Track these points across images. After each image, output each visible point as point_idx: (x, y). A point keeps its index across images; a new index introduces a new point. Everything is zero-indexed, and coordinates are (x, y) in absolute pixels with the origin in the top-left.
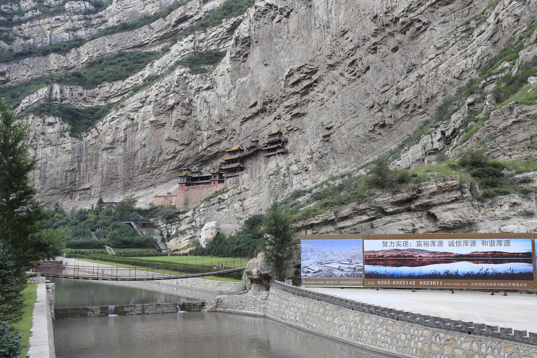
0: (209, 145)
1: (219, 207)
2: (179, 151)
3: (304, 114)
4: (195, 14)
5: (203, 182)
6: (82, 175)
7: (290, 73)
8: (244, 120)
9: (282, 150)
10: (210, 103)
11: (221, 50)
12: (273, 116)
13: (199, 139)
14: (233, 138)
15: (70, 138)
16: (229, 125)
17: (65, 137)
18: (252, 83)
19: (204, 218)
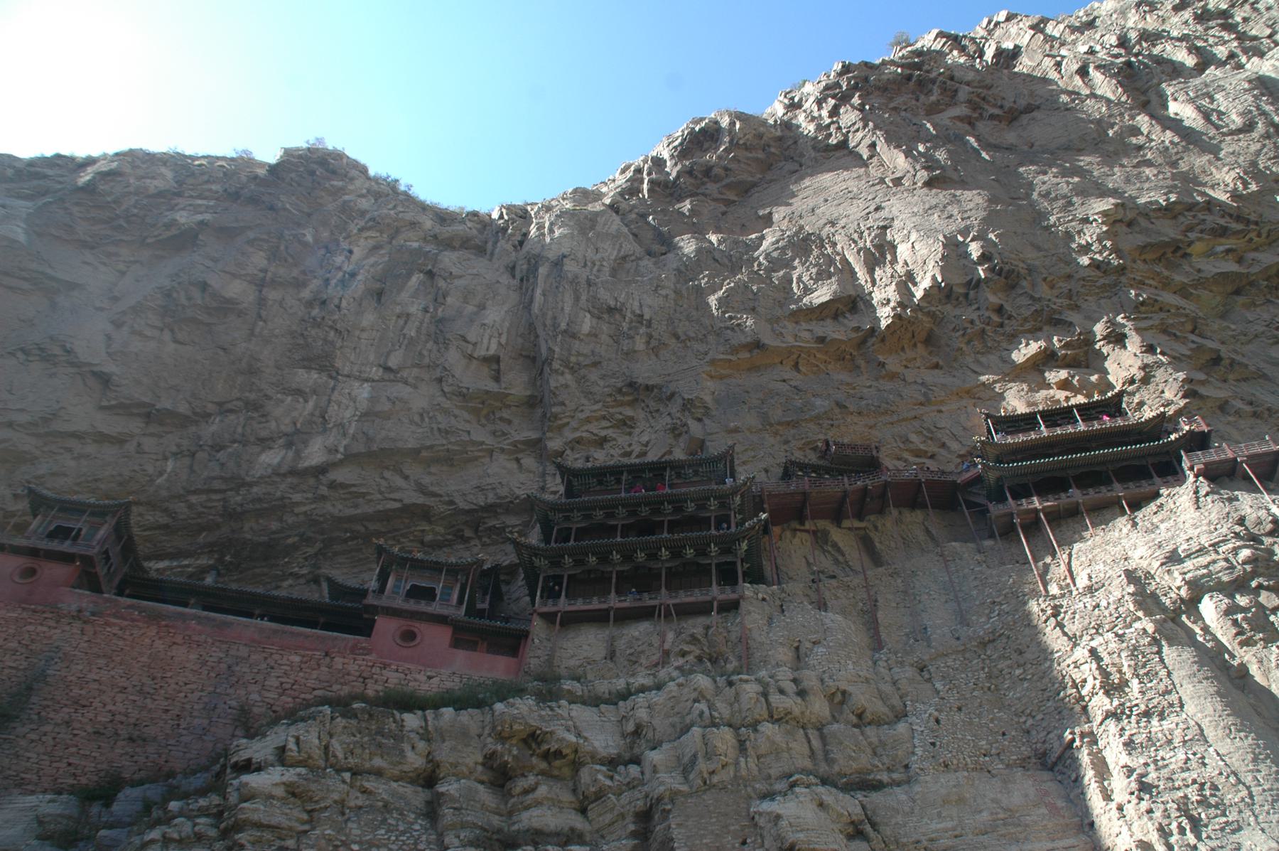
0: (360, 448)
1: (496, 821)
10: (457, 282)
13: (285, 414)
14: (602, 442)
16: (594, 376)
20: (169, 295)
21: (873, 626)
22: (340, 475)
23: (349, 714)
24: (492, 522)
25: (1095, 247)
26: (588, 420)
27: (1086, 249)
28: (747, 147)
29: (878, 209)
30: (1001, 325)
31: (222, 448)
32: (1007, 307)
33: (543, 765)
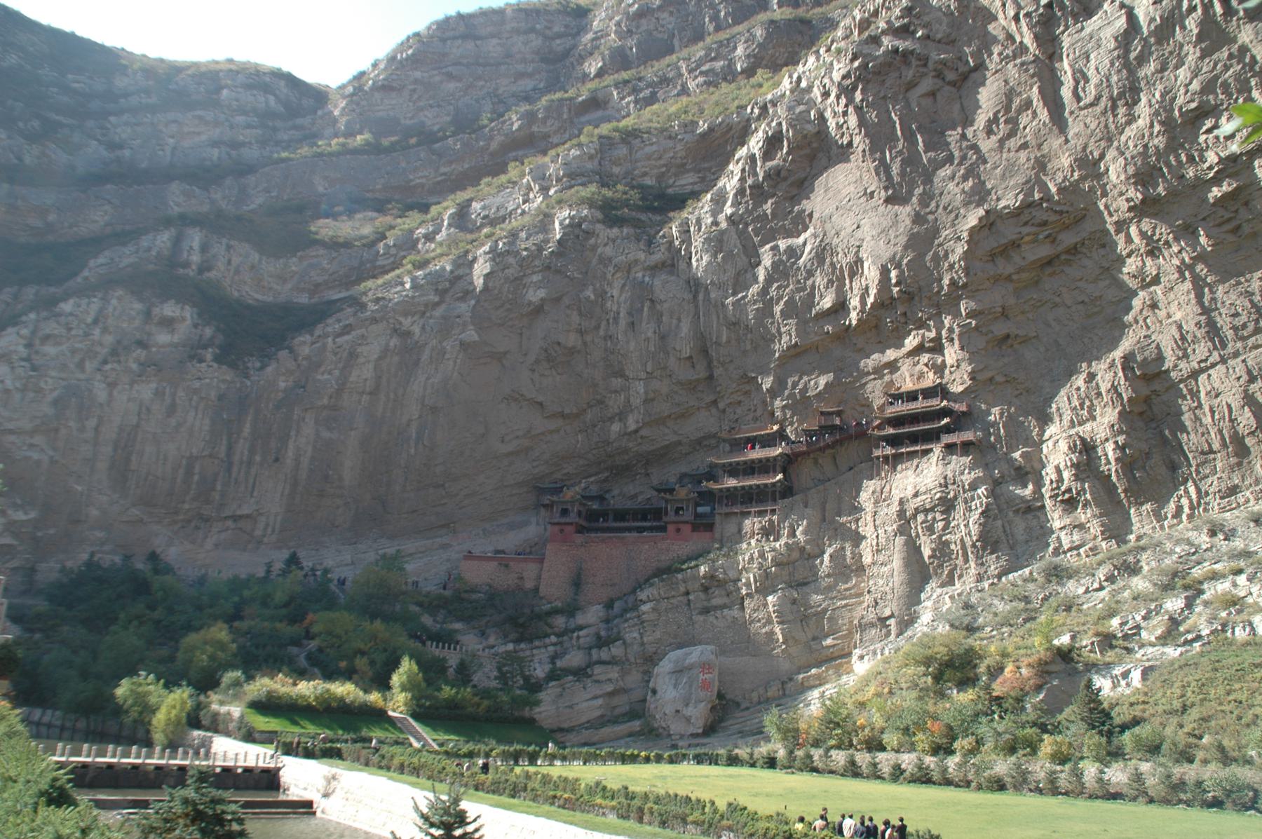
1: (705, 603)
2: (543, 434)
3: (1025, 340)
4: (555, 132)
5: (626, 524)
6: (234, 475)
7: (984, 222)
8: (793, 352)
9: (968, 436)
10: (666, 305)
11: (670, 191)
12: (911, 342)
13: (615, 403)
15: (215, 365)
17: (201, 361)
18: (822, 254)
19: (658, 634)
20: (546, 351)
21: (824, 510)
22: (643, 432)
23: (663, 580)
24: (705, 443)
25: (956, 266)
26: (732, 393)
27: (951, 266)
28: (799, 147)
29: (858, 227)
30: (906, 323)
31: (595, 426)
32: (908, 314)
33: (716, 583)
